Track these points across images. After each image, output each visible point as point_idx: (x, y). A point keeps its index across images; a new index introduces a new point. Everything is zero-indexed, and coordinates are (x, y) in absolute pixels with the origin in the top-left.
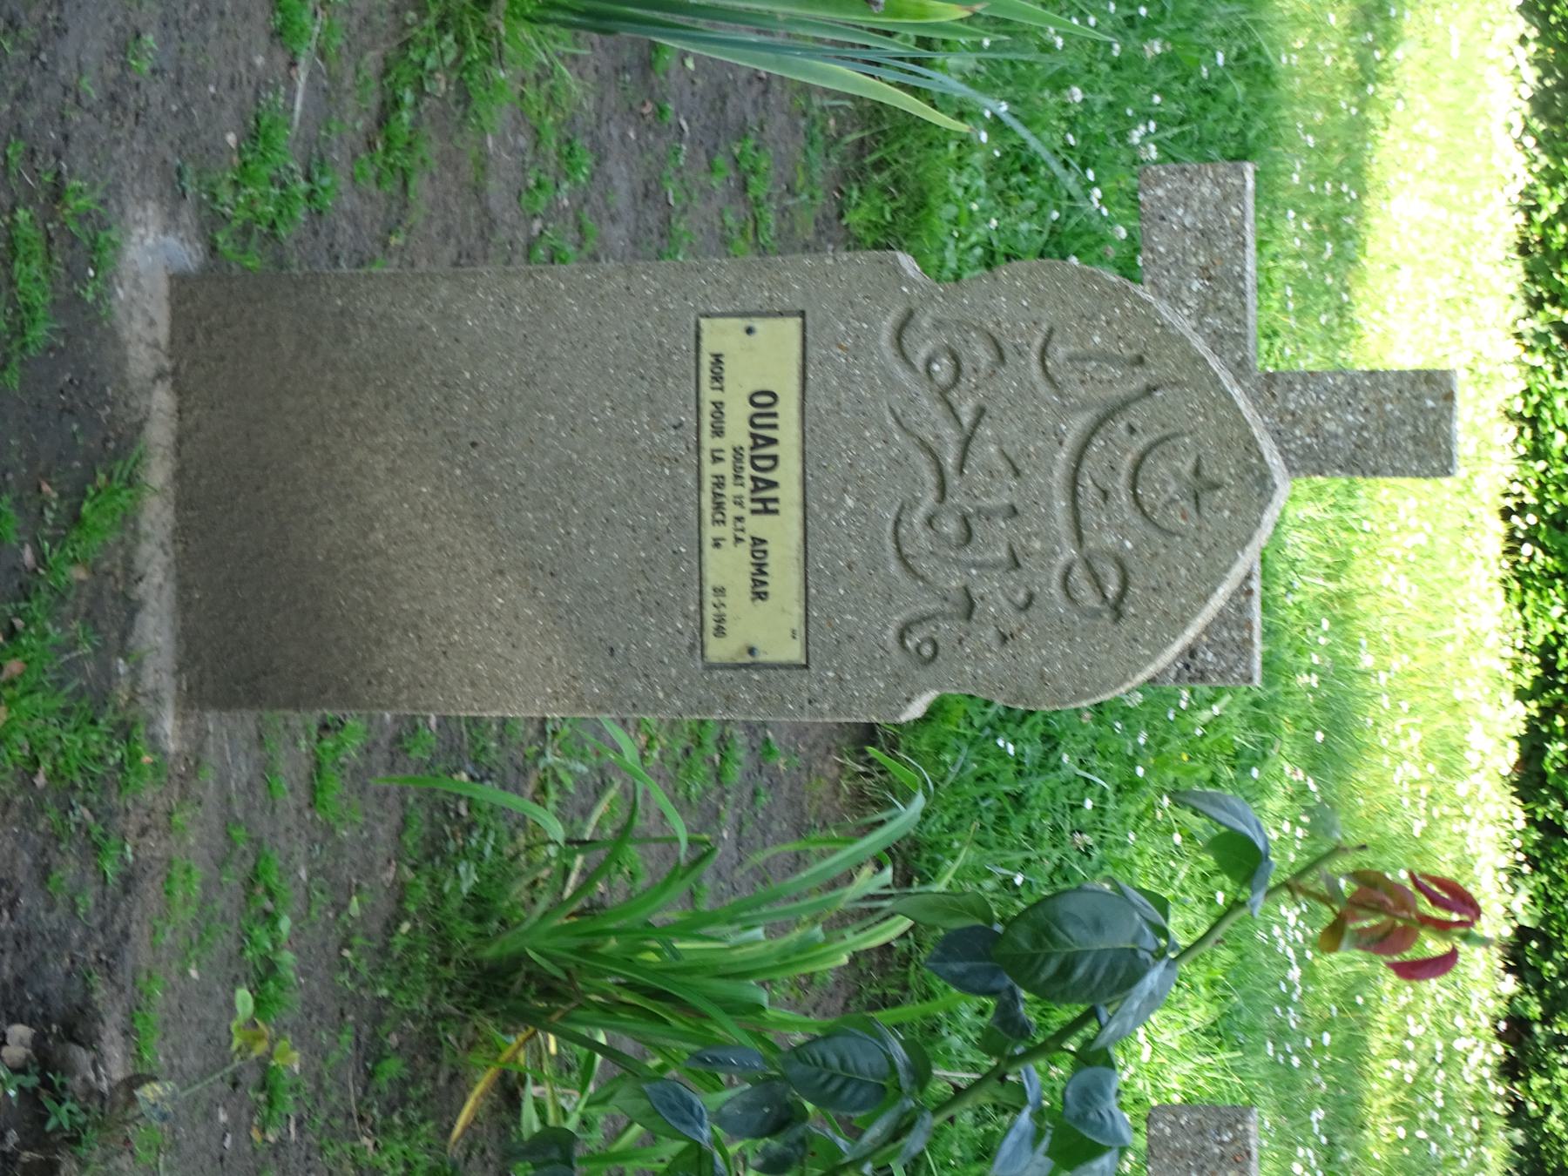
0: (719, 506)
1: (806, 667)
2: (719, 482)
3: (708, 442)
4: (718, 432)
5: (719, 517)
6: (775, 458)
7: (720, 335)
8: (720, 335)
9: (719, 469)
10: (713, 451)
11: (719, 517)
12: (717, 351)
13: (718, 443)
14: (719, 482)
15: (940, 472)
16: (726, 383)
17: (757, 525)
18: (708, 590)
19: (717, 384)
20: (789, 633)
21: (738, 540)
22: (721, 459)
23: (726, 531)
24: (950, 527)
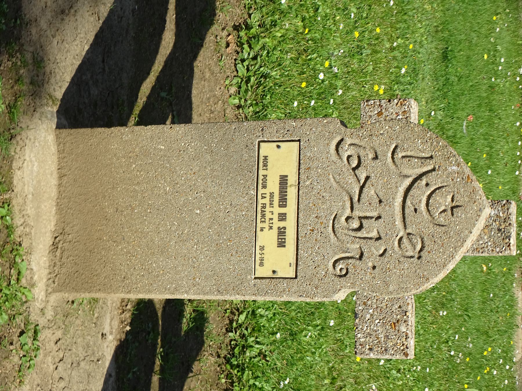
0: (263, 216)
1: (296, 277)
2: (264, 206)
5: (263, 220)
7: (266, 149)
8: (266, 149)
10: (262, 194)
11: (263, 220)
18: (258, 248)
19: (264, 168)
21: (271, 228)
22: (265, 197)
23: (266, 225)
24: (355, 224)
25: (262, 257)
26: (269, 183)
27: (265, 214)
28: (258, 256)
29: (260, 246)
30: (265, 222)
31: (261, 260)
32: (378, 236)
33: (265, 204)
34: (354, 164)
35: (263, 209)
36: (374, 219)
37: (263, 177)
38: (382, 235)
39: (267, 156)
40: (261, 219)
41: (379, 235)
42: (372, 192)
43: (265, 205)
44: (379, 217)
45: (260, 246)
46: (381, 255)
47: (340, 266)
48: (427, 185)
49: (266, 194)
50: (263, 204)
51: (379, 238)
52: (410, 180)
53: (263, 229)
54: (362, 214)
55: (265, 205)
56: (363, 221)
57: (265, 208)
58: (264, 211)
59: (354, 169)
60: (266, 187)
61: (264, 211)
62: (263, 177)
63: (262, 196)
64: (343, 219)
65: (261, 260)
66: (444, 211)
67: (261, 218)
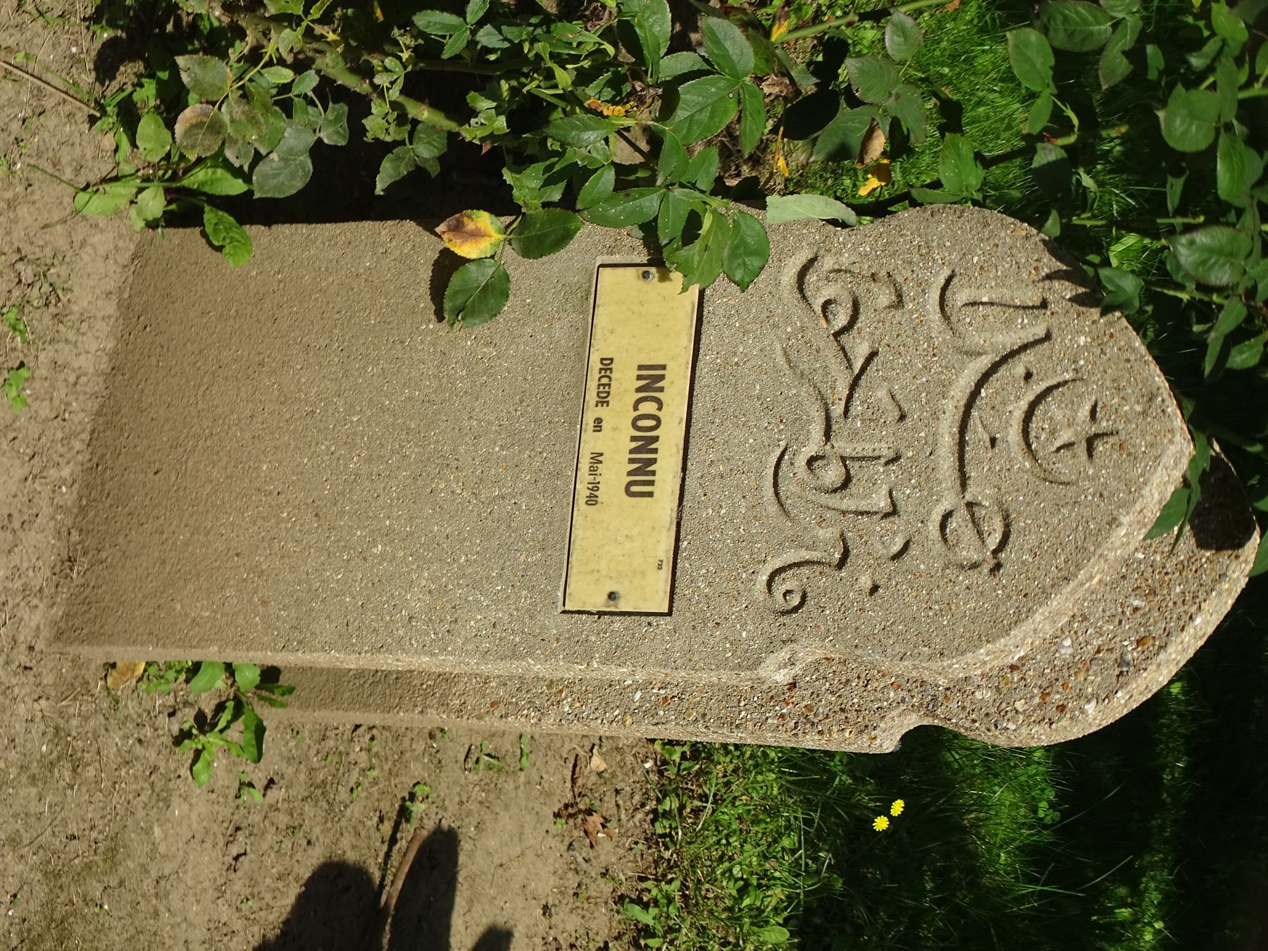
15: (828, 419)
32: (889, 509)
34: (841, 320)
36: (883, 461)
38: (901, 505)
41: (893, 504)
42: (882, 393)
44: (896, 459)
46: (897, 556)
47: (789, 582)
48: (1028, 376)
51: (894, 512)
52: (984, 362)
54: (848, 452)
56: (854, 467)
59: (837, 335)
64: (801, 461)
66: (1068, 446)
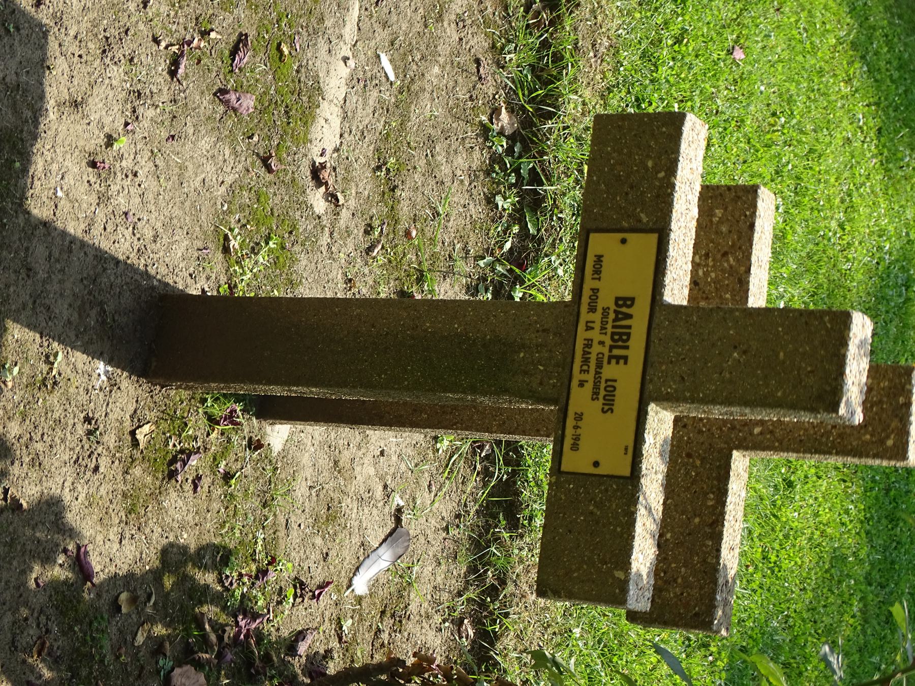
0: (586, 361)
2: (589, 344)
3: (585, 316)
4: (592, 309)
5: (585, 368)
6: (629, 327)
9: (589, 334)
10: (587, 322)
11: (585, 368)
12: (598, 253)
13: (591, 317)
14: (589, 344)
16: (602, 275)
17: (610, 371)
19: (596, 276)
20: (624, 452)
22: (593, 328)
25: (578, 433)
26: (600, 305)
27: (590, 358)
28: (569, 431)
29: (576, 413)
30: (588, 371)
31: (575, 439)
33: (592, 340)
35: (587, 349)
37: (592, 293)
39: (602, 256)
40: (581, 366)
43: (590, 342)
45: (576, 413)
49: (593, 322)
50: (588, 340)
53: (586, 384)
55: (590, 342)
57: (590, 348)
58: (590, 353)
60: (596, 309)
61: (590, 353)
62: (592, 293)
63: (587, 326)
65: (575, 439)
67: (581, 364)
